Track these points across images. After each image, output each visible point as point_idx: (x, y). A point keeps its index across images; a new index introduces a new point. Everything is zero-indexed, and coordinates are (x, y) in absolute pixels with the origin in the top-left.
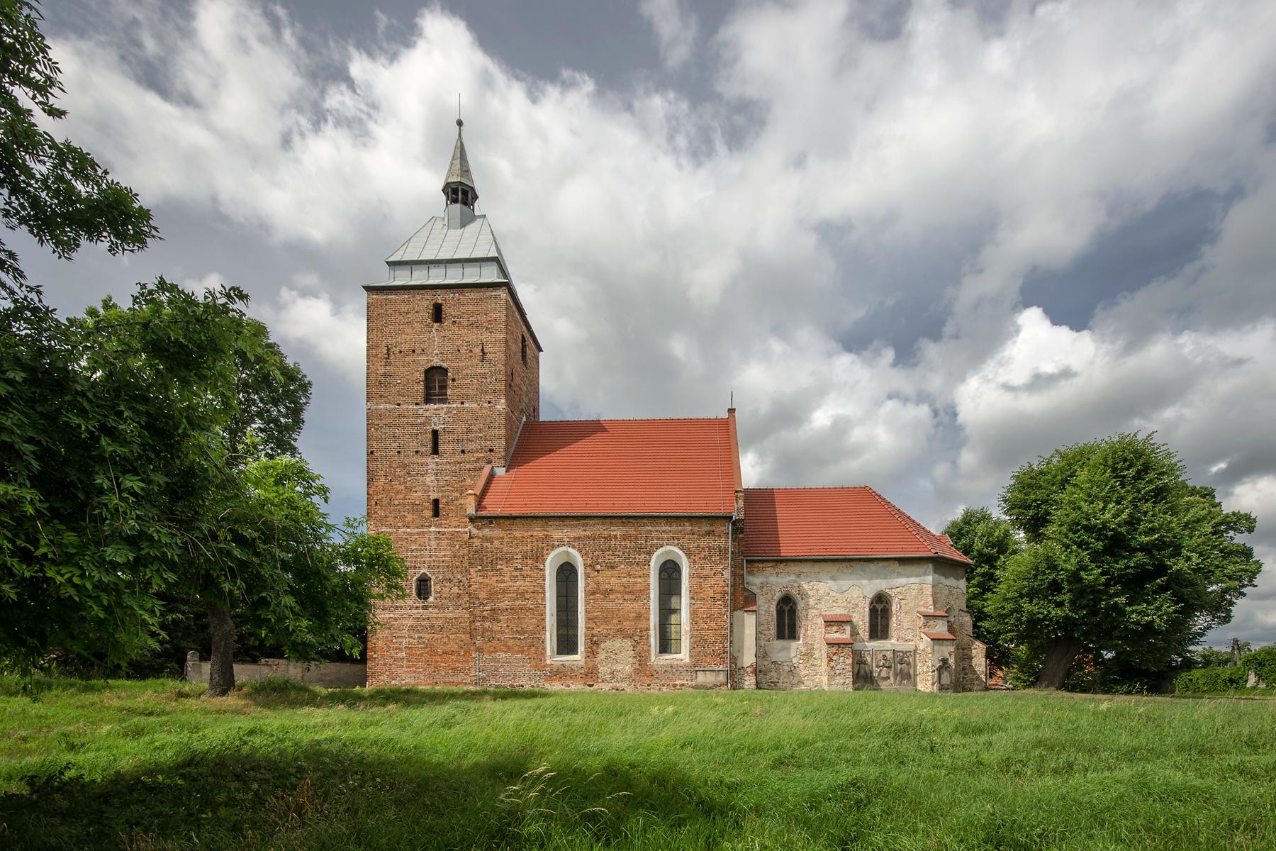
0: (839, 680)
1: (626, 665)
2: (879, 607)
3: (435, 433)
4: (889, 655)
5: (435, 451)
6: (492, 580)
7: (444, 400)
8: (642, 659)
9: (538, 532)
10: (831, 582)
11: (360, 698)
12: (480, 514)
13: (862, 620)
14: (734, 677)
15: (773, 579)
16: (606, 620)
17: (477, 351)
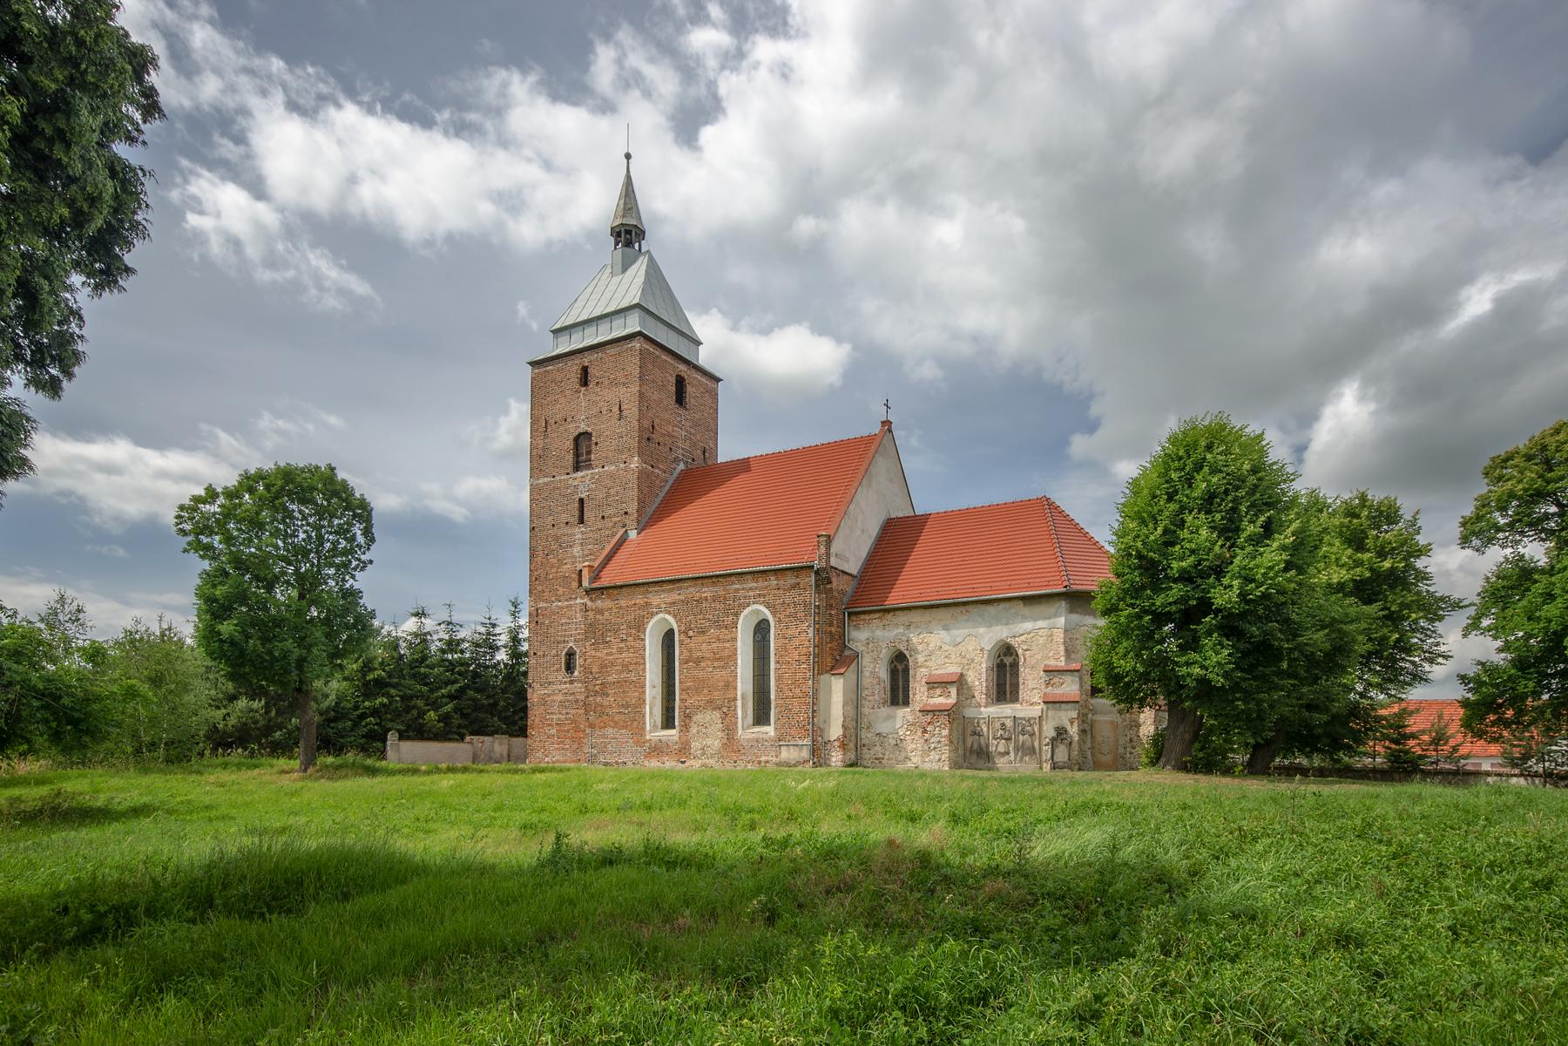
0: (934, 756)
1: (715, 742)
2: (1008, 660)
3: (581, 500)
4: (1009, 723)
5: (581, 521)
6: (602, 654)
7: (589, 467)
8: (729, 730)
9: (640, 600)
10: (943, 633)
11: (523, 771)
12: (594, 585)
13: (979, 678)
14: (818, 754)
15: (879, 633)
16: (698, 691)
17: (616, 409)
